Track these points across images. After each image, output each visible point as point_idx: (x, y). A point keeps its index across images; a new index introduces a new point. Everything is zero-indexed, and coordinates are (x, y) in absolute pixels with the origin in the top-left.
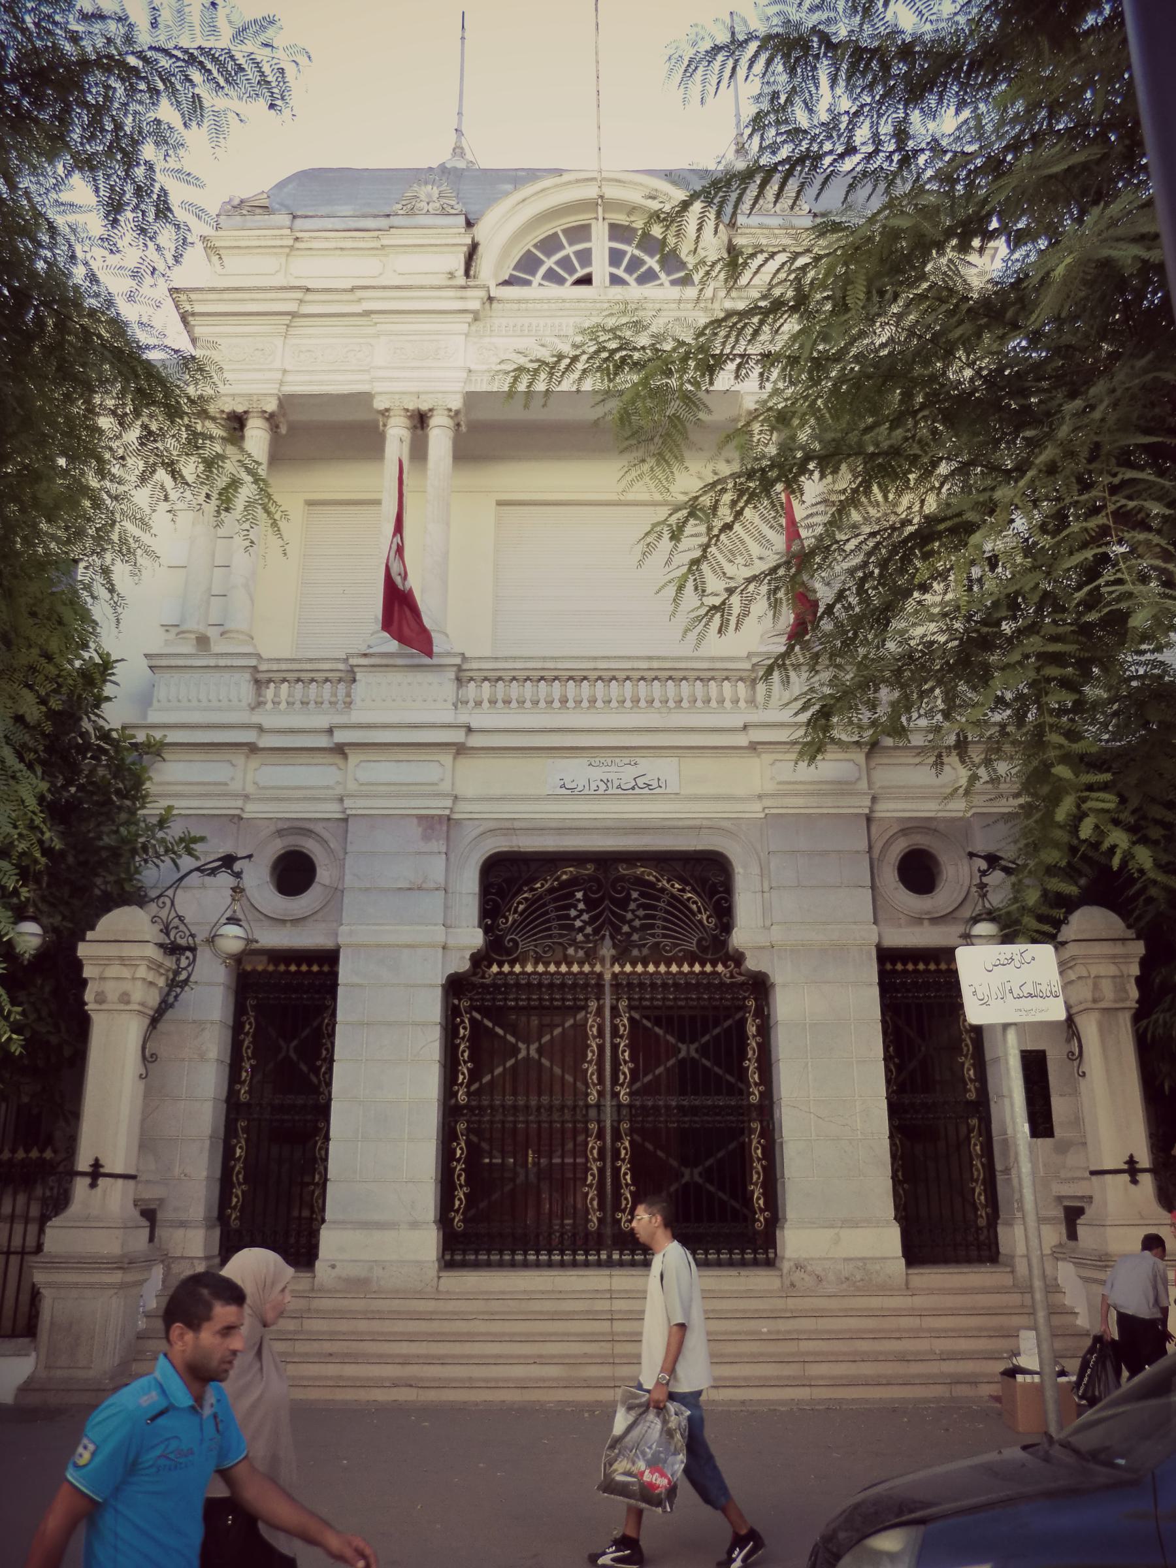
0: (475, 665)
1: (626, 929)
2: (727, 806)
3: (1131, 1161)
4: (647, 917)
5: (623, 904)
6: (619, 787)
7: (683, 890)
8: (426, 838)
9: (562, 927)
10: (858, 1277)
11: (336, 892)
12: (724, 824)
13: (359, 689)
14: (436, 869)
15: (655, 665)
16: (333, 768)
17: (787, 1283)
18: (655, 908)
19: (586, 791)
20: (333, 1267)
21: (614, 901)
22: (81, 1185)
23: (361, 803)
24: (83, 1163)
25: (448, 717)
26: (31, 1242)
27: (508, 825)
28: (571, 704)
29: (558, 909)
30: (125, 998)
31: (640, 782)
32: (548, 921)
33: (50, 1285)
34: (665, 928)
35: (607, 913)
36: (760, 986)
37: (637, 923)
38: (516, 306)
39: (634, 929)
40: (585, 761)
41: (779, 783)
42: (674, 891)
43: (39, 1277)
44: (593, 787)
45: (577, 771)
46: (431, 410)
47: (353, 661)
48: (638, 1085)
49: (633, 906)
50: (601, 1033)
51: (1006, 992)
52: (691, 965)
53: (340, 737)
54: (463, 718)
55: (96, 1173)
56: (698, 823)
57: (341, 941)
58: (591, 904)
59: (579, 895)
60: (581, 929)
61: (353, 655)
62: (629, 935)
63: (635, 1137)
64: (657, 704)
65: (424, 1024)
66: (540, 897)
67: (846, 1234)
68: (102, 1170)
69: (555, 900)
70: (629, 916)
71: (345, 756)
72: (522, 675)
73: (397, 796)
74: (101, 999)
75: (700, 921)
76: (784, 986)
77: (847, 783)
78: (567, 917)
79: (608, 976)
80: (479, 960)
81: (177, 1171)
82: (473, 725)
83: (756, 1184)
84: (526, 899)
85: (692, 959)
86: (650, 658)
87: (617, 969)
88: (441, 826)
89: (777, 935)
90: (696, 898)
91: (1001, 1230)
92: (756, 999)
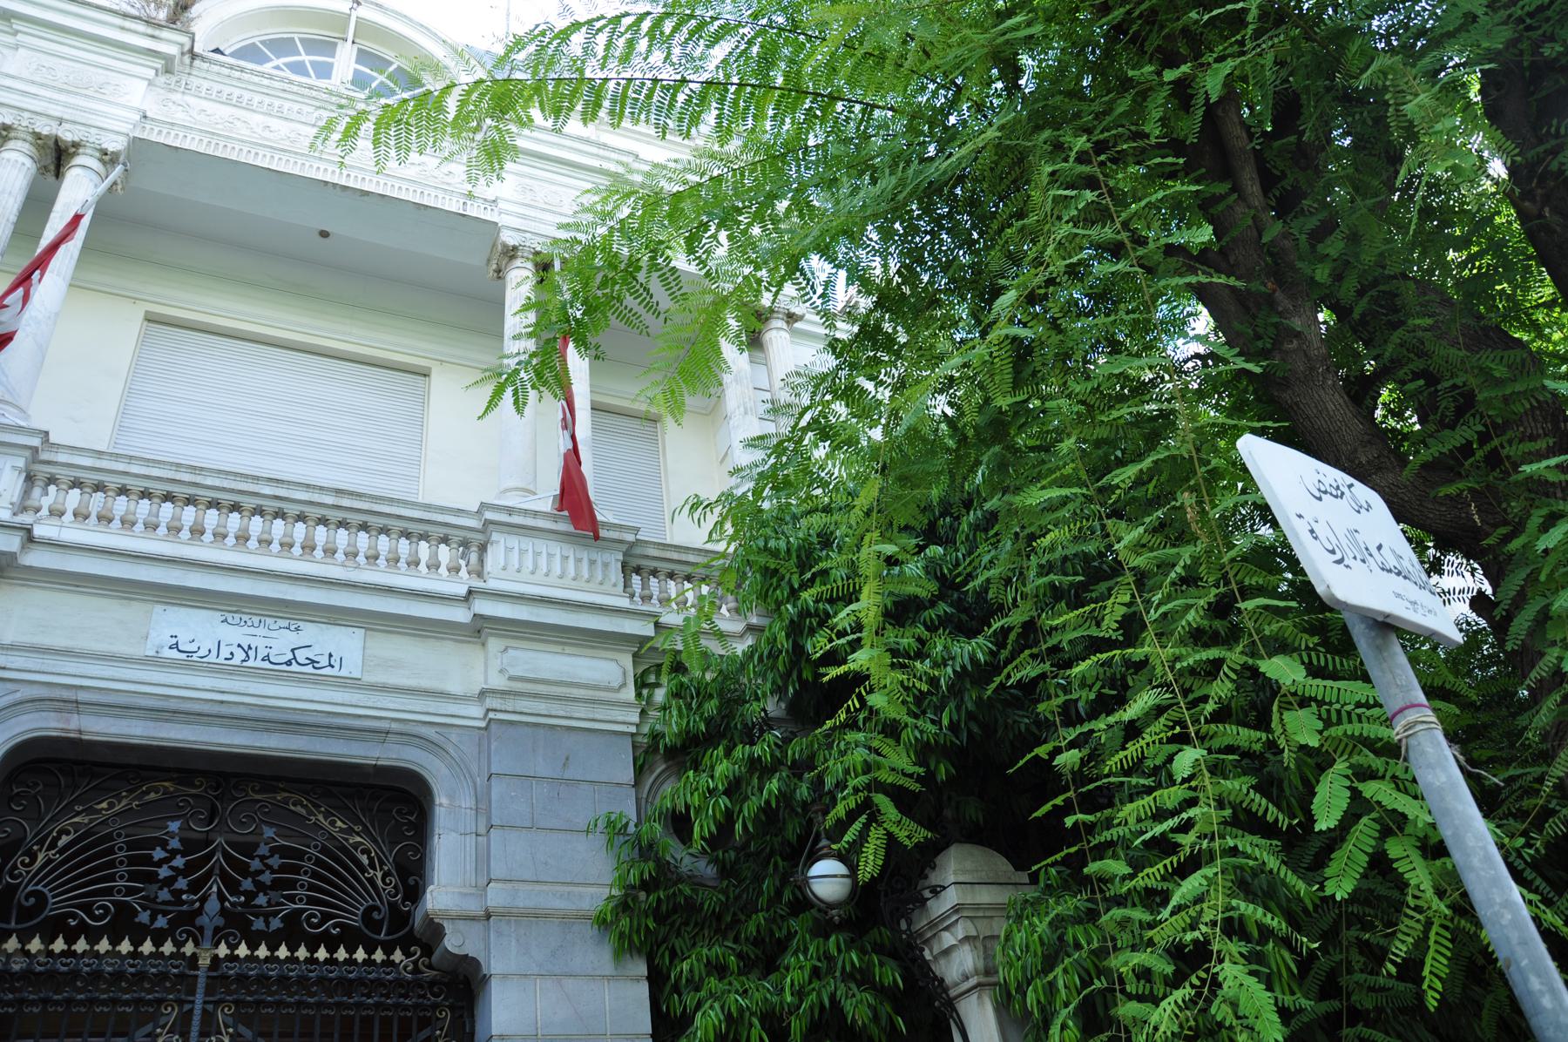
0: (62, 457)
4: (283, 868)
6: (266, 658)
7: (350, 831)
9: (133, 876)
12: (424, 731)
15: (346, 502)
19: (212, 658)
27: (66, 694)
31: (301, 656)
32: (111, 864)
34: (312, 888)
35: (219, 856)
36: (464, 985)
37: (267, 878)
38: (226, 71)
39: (261, 887)
41: (511, 678)
44: (225, 653)
46: (76, 145)
49: (263, 850)
52: (351, 950)
56: (384, 725)
60: (169, 881)
62: (250, 896)
70: (256, 864)
72: (136, 485)
75: (371, 881)
76: (505, 976)
77: (608, 689)
78: (148, 860)
79: (205, 961)
85: (350, 938)
86: (339, 492)
89: (496, 897)
90: (368, 844)
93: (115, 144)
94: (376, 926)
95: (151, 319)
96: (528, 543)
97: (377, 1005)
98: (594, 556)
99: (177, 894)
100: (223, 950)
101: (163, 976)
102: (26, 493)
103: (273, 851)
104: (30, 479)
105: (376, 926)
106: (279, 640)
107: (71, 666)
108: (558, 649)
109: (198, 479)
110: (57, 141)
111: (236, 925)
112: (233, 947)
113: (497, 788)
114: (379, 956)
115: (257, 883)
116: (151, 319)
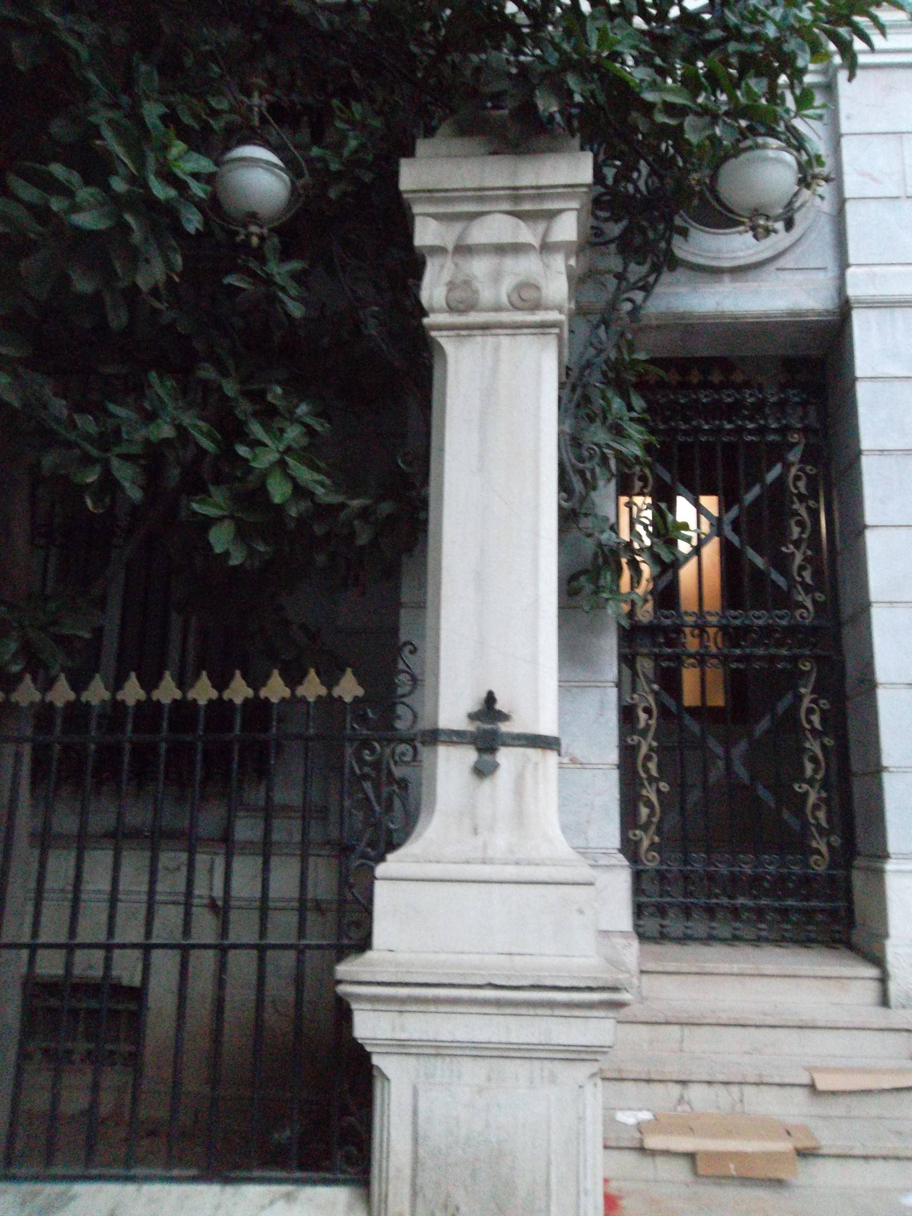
22: (451, 767)
24: (453, 708)
43: (367, 1026)
55: (488, 731)
68: (504, 727)
74: (463, 300)
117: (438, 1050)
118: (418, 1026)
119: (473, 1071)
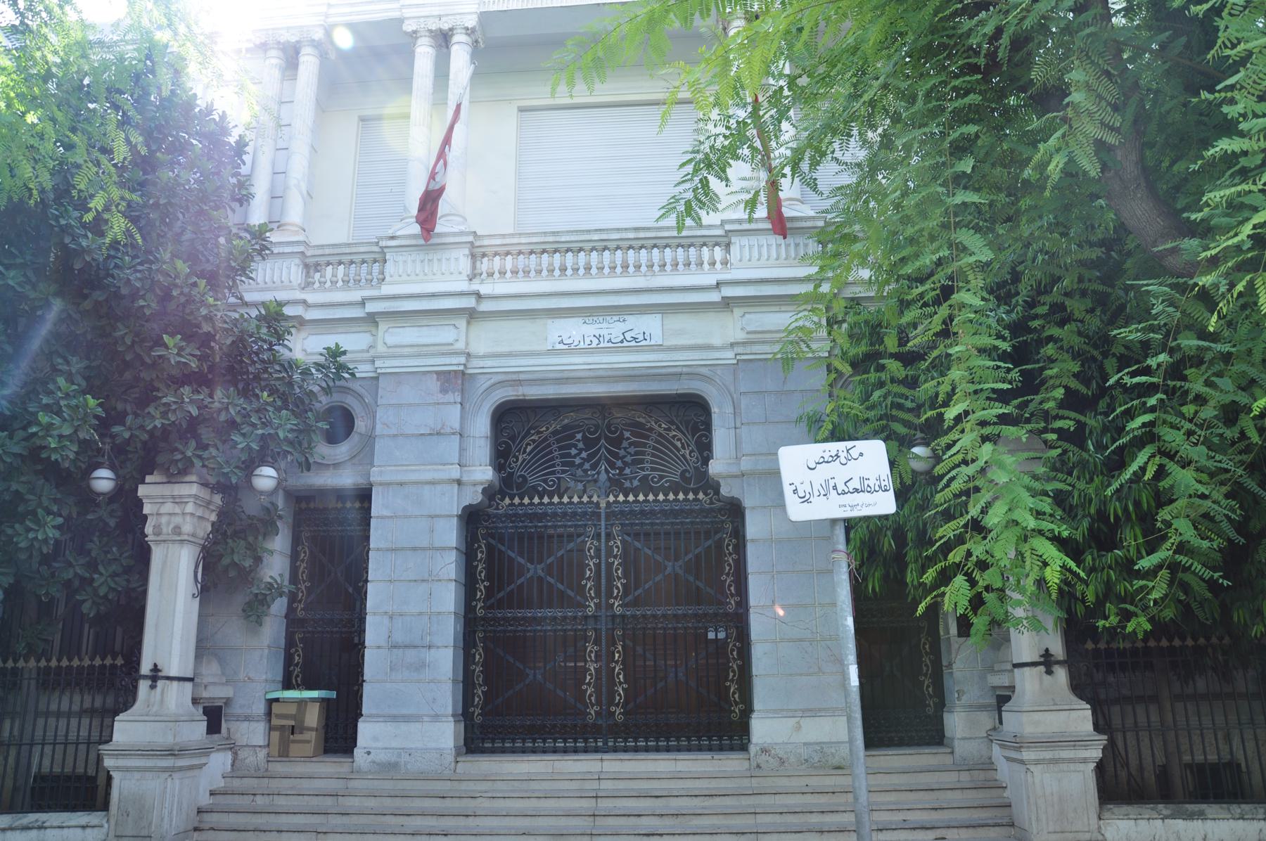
0: (486, 242)
1: (619, 463)
2: (704, 355)
3: (1047, 654)
4: (637, 453)
5: (617, 442)
6: (610, 341)
7: (669, 429)
8: (444, 391)
9: (564, 464)
10: (816, 759)
11: (370, 439)
13: (390, 268)
14: (453, 416)
15: (642, 235)
16: (368, 335)
17: (754, 764)
18: (644, 445)
20: (369, 753)
21: (607, 438)
22: (143, 686)
23: (388, 363)
24: (145, 668)
25: (464, 286)
26: (95, 735)
27: (515, 377)
28: (569, 272)
29: (560, 448)
30: (177, 530)
31: (628, 336)
32: (552, 459)
33: (118, 769)
35: (603, 450)
36: (735, 510)
37: (628, 459)
39: (626, 464)
40: (580, 320)
42: (661, 431)
43: (108, 763)
45: (575, 331)
46: (451, 29)
47: (383, 243)
48: (630, 597)
49: (625, 444)
50: (598, 556)
51: (829, 488)
52: (676, 494)
53: (371, 307)
54: (475, 286)
55: (156, 675)
56: (679, 370)
57: (372, 479)
58: (589, 443)
59: (579, 436)
60: (581, 465)
61: (382, 238)
62: (622, 469)
63: (628, 642)
64: (644, 269)
65: (444, 549)
66: (546, 439)
67: (807, 723)
69: (558, 441)
70: (622, 452)
71: (376, 324)
73: (419, 356)
75: (683, 456)
76: (753, 508)
78: (569, 455)
79: (603, 505)
80: (490, 493)
81: (242, 676)
82: (482, 292)
83: (732, 681)
84: (534, 441)
86: (636, 229)
87: (611, 499)
88: (456, 381)
89: (746, 464)
90: (680, 435)
91: (946, 716)
92: (732, 522)
93: (471, 22)
94: (688, 481)
95: (522, 110)
96: (754, 240)
97: (692, 523)
98: (797, 241)
99: (585, 471)
100: (611, 499)
101: (585, 513)
102: (474, 267)
103: (631, 444)
104: (473, 256)
105: (688, 481)
106: (614, 329)
107: (513, 362)
108: (777, 309)
109: (558, 239)
110: (441, 30)
111: (616, 485)
112: (616, 496)
113: (744, 402)
114: (691, 496)
115: (624, 463)
116: (522, 110)
117: (127, 769)
118: (121, 762)
119: (137, 775)
